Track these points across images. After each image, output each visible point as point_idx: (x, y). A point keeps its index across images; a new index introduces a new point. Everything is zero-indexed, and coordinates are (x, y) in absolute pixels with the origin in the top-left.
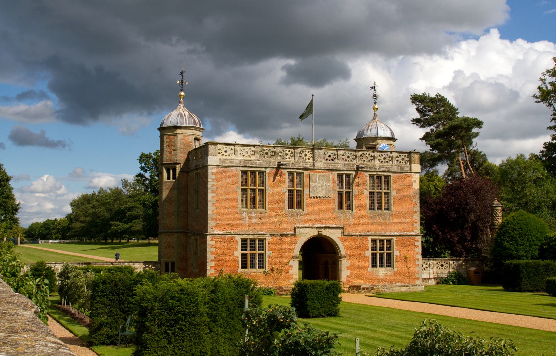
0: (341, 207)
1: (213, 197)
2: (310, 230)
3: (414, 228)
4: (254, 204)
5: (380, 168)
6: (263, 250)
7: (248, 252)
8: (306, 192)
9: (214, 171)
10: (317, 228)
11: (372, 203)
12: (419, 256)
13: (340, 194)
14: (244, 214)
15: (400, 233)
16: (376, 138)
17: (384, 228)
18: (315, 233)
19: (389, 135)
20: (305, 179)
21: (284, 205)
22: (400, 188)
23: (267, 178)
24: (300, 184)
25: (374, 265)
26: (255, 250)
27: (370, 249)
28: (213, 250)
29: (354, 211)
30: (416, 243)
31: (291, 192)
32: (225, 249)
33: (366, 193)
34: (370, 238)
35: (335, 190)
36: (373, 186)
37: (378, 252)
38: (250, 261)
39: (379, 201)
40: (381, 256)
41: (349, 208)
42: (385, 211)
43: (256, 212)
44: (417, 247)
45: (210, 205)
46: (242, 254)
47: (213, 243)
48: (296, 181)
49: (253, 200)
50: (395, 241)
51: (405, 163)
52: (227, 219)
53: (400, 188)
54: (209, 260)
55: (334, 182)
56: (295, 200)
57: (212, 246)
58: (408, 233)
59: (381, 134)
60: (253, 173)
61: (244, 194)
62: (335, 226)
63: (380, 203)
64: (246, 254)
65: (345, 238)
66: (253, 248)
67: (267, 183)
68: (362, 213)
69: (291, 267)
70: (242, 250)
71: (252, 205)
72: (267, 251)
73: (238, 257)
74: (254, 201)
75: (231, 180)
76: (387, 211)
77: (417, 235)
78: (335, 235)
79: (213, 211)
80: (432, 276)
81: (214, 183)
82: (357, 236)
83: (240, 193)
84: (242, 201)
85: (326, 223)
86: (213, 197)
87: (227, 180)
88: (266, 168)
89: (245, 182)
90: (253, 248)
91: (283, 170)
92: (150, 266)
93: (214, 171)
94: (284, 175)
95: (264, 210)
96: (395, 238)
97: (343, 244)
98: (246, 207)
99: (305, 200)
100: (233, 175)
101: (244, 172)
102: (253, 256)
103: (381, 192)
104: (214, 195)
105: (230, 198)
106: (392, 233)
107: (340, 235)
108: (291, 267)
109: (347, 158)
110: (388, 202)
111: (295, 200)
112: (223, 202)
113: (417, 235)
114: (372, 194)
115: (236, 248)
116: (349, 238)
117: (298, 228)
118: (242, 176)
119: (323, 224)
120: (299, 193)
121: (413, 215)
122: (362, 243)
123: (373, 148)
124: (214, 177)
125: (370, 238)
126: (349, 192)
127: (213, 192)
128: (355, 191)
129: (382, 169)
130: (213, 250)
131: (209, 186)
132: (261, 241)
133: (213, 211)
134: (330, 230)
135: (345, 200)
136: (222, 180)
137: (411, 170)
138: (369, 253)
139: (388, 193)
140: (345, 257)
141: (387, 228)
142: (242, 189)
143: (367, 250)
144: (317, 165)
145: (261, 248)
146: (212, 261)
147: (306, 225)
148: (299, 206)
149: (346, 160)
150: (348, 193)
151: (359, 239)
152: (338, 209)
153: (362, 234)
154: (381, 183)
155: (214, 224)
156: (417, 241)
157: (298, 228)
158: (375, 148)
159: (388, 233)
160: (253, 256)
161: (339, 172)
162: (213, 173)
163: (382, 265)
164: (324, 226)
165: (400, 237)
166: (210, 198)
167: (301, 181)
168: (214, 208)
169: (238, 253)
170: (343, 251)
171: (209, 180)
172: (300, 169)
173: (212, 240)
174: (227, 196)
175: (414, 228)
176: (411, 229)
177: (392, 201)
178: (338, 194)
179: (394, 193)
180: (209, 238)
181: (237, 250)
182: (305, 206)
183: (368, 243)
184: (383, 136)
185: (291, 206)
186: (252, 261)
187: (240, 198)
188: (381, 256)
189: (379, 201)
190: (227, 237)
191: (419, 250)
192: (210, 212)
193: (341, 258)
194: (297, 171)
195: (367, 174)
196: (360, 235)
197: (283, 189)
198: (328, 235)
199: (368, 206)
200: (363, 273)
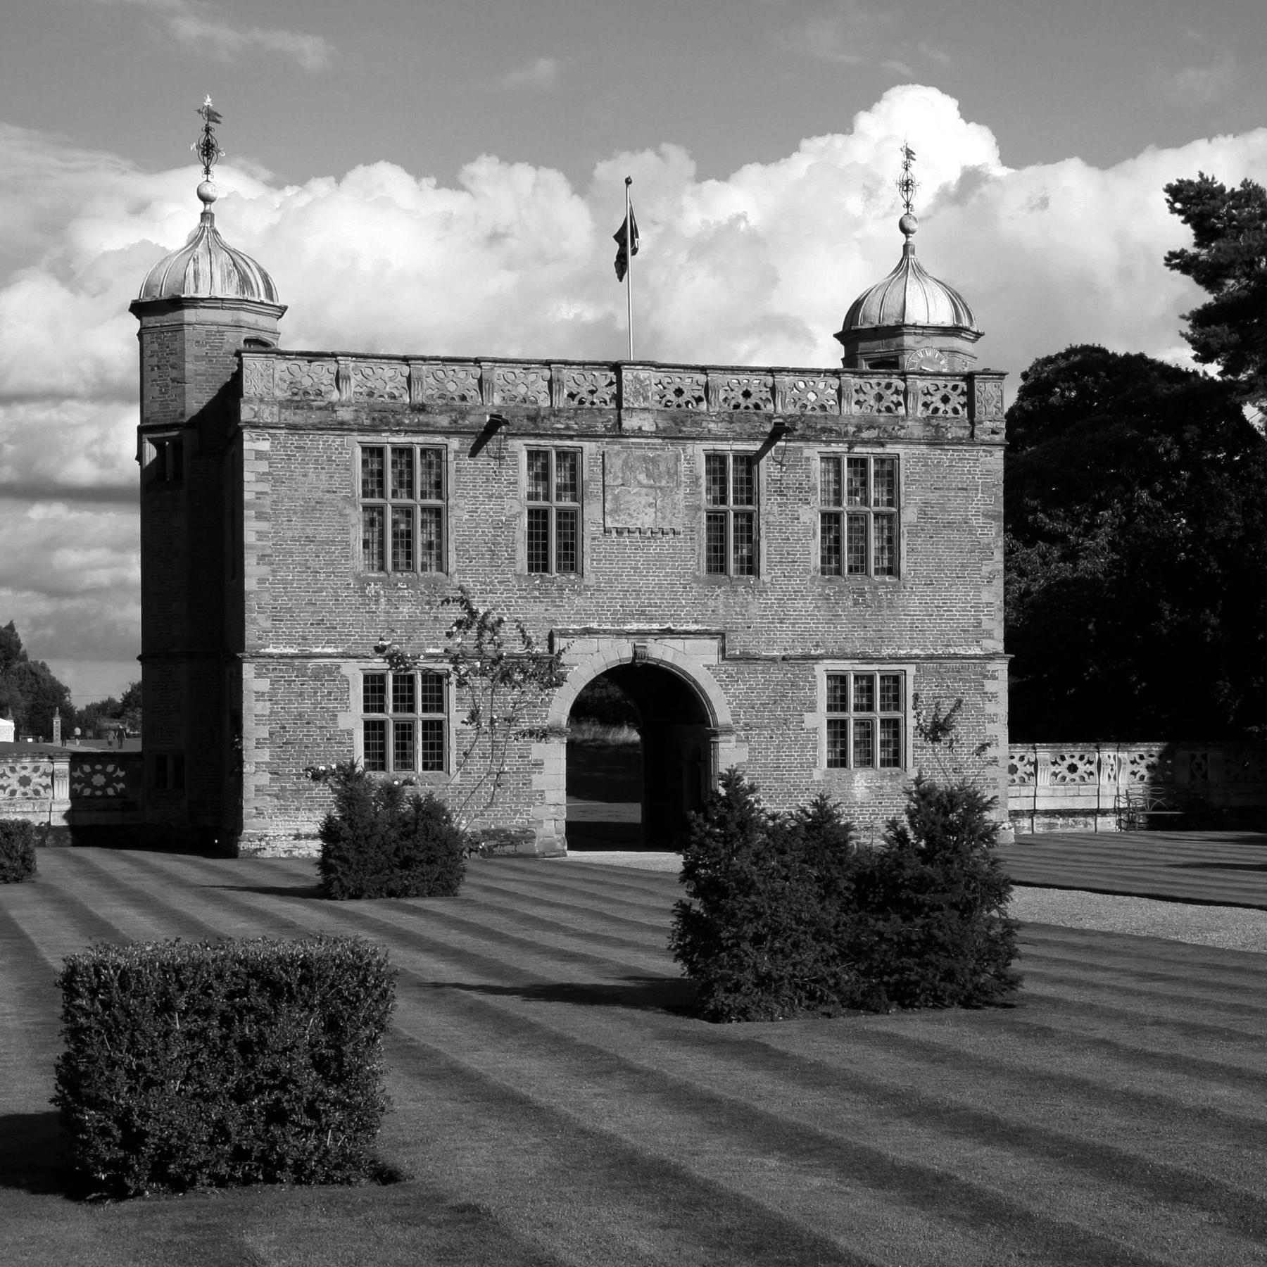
0: (717, 563)
1: (261, 535)
2: (605, 643)
3: (979, 634)
4: (409, 556)
5: (859, 429)
6: (440, 709)
7: (389, 715)
8: (592, 514)
9: (264, 446)
10: (629, 634)
11: (832, 550)
12: (1000, 730)
13: (716, 521)
16: (898, 330)
17: (870, 634)
18: (621, 652)
19: (943, 315)
20: (588, 470)
21: (512, 559)
22: (932, 497)
23: (452, 467)
24: (573, 487)
25: (839, 761)
26: (411, 709)
27: (822, 703)
28: (263, 708)
30: (990, 686)
31: (538, 518)
32: (307, 706)
33: (811, 516)
34: (821, 671)
35: (698, 508)
36: (838, 493)
37: (852, 716)
38: (397, 746)
39: (859, 545)
40: (866, 728)
41: (750, 566)
42: (877, 578)
43: (411, 585)
44: (994, 696)
45: (250, 562)
46: (368, 725)
47: (264, 685)
48: (555, 480)
49: (405, 540)
50: (910, 681)
51: (955, 411)
52: (310, 608)
53: (932, 497)
54: (248, 744)
55: (695, 481)
56: (553, 542)
57: (260, 695)
58: (961, 651)
59: (916, 315)
60: (403, 452)
61: (372, 523)
62: (694, 627)
63: (860, 551)
64: (382, 724)
65: (732, 669)
66: (405, 701)
67: (451, 484)
69: (539, 764)
70: (366, 709)
71: (402, 560)
72: (453, 714)
73: (350, 733)
74: (409, 545)
75: (323, 477)
76: (887, 578)
77: (990, 657)
78: (694, 659)
79: (262, 581)
80: (1108, 804)
81: (266, 487)
82: (773, 659)
83: (357, 518)
84: (366, 544)
85: (662, 620)
86: (261, 535)
87: (312, 476)
89: (374, 483)
90: (405, 701)
91: (510, 442)
92: (110, 768)
93: (264, 446)
94: (514, 455)
95: (442, 575)
96: (911, 669)
97: (725, 688)
98: (382, 568)
99: (587, 542)
100: (330, 460)
101: (374, 452)
102: (404, 731)
103: (866, 515)
104: (264, 526)
105: (322, 535)
107: (714, 659)
108: (539, 764)
109: (741, 400)
110: (891, 543)
111: (553, 542)
112: (296, 547)
113: (990, 657)
114: (830, 520)
115: (344, 701)
116: (745, 668)
117: (564, 634)
118: (365, 463)
119: (651, 620)
120: (569, 520)
121: (977, 588)
122: (794, 685)
123: (889, 364)
124: (263, 466)
125: (821, 671)
126: (749, 516)
127: (260, 516)
128: (769, 508)
130: (263, 708)
131: (248, 496)
132: (435, 683)
133: (262, 581)
134: (677, 644)
136: (291, 478)
137: (972, 435)
138: (819, 719)
139: (890, 517)
140: (729, 731)
141: (885, 634)
142: (365, 508)
143: (812, 708)
144: (629, 423)
145: (435, 700)
146: (259, 744)
148: (570, 559)
149: (737, 407)
151: (776, 673)
152: (709, 570)
153: (791, 653)
154: (864, 484)
155: (267, 624)
156: (994, 678)
157: (564, 634)
158: (895, 364)
159: (886, 652)
160: (404, 731)
161: (710, 446)
162: (260, 455)
163: (866, 761)
164: (656, 626)
165: (930, 665)
166: (250, 537)
167: (573, 477)
168: (265, 570)
169: (353, 718)
170: (722, 712)
171: (248, 476)
172: (571, 437)
173: (258, 676)
174: (310, 531)
175: (979, 634)
177: (903, 543)
178: (709, 518)
179: (909, 515)
180: (248, 670)
181: (347, 709)
182: (587, 562)
183: (813, 687)
184: (922, 321)
185: (538, 562)
186: (404, 747)
187: (358, 534)
188: (866, 728)
189: (859, 545)
190: (311, 664)
191: (1000, 708)
192: (250, 584)
193: (715, 734)
194: (557, 442)
195: (813, 451)
196: (784, 659)
197: (507, 503)
198: (668, 659)
199: (816, 560)
200: (796, 787)
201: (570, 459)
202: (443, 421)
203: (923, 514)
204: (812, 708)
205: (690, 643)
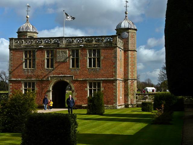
14: (25, 71)
15: (105, 79)
29: (80, 68)
41: (78, 66)
60: (30, 52)
68: (84, 69)
88: (35, 49)
96: (102, 82)
106: (100, 79)
114: (90, 59)
119: (63, 75)
128: (80, 58)
129: (95, 46)
130: (11, 87)
132: (34, 84)
135: (76, 63)
146: (10, 92)
147: (55, 75)
150: (77, 60)
159: (98, 79)
176: (111, 77)
179: (102, 58)
201: (52, 51)
202: (35, 47)
203: (104, 57)
204: (86, 87)
205: (68, 78)
